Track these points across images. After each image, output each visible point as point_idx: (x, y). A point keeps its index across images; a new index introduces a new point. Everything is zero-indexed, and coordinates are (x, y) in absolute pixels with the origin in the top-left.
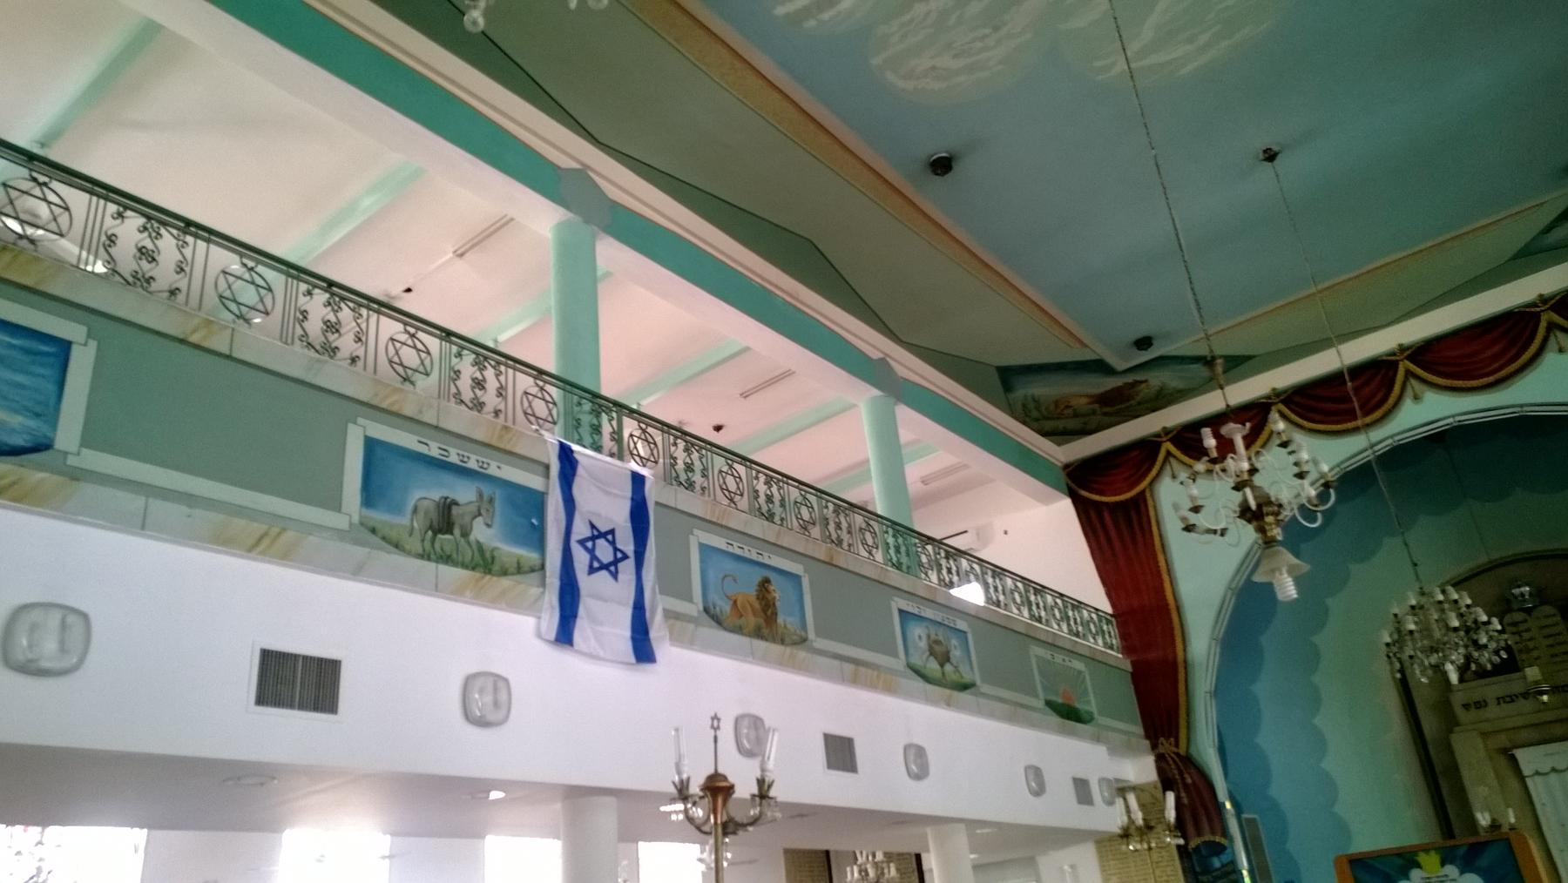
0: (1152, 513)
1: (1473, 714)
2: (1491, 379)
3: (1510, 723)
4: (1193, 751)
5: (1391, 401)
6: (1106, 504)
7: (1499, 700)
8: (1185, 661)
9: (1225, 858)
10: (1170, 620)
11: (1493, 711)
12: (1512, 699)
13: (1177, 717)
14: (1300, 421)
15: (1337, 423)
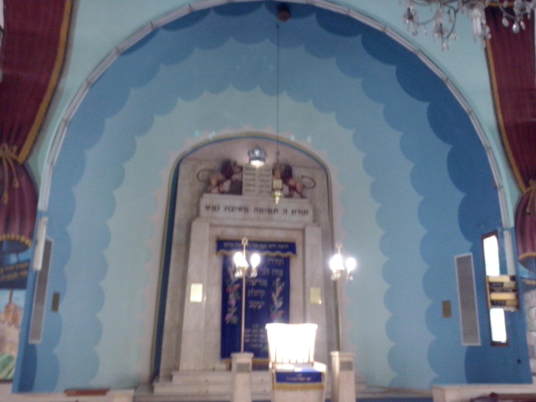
1: (210, 213)
3: (227, 222)
4: (31, 161)
8: (55, 89)
9: (23, 256)
10: (55, 52)
11: (221, 214)
12: (232, 209)
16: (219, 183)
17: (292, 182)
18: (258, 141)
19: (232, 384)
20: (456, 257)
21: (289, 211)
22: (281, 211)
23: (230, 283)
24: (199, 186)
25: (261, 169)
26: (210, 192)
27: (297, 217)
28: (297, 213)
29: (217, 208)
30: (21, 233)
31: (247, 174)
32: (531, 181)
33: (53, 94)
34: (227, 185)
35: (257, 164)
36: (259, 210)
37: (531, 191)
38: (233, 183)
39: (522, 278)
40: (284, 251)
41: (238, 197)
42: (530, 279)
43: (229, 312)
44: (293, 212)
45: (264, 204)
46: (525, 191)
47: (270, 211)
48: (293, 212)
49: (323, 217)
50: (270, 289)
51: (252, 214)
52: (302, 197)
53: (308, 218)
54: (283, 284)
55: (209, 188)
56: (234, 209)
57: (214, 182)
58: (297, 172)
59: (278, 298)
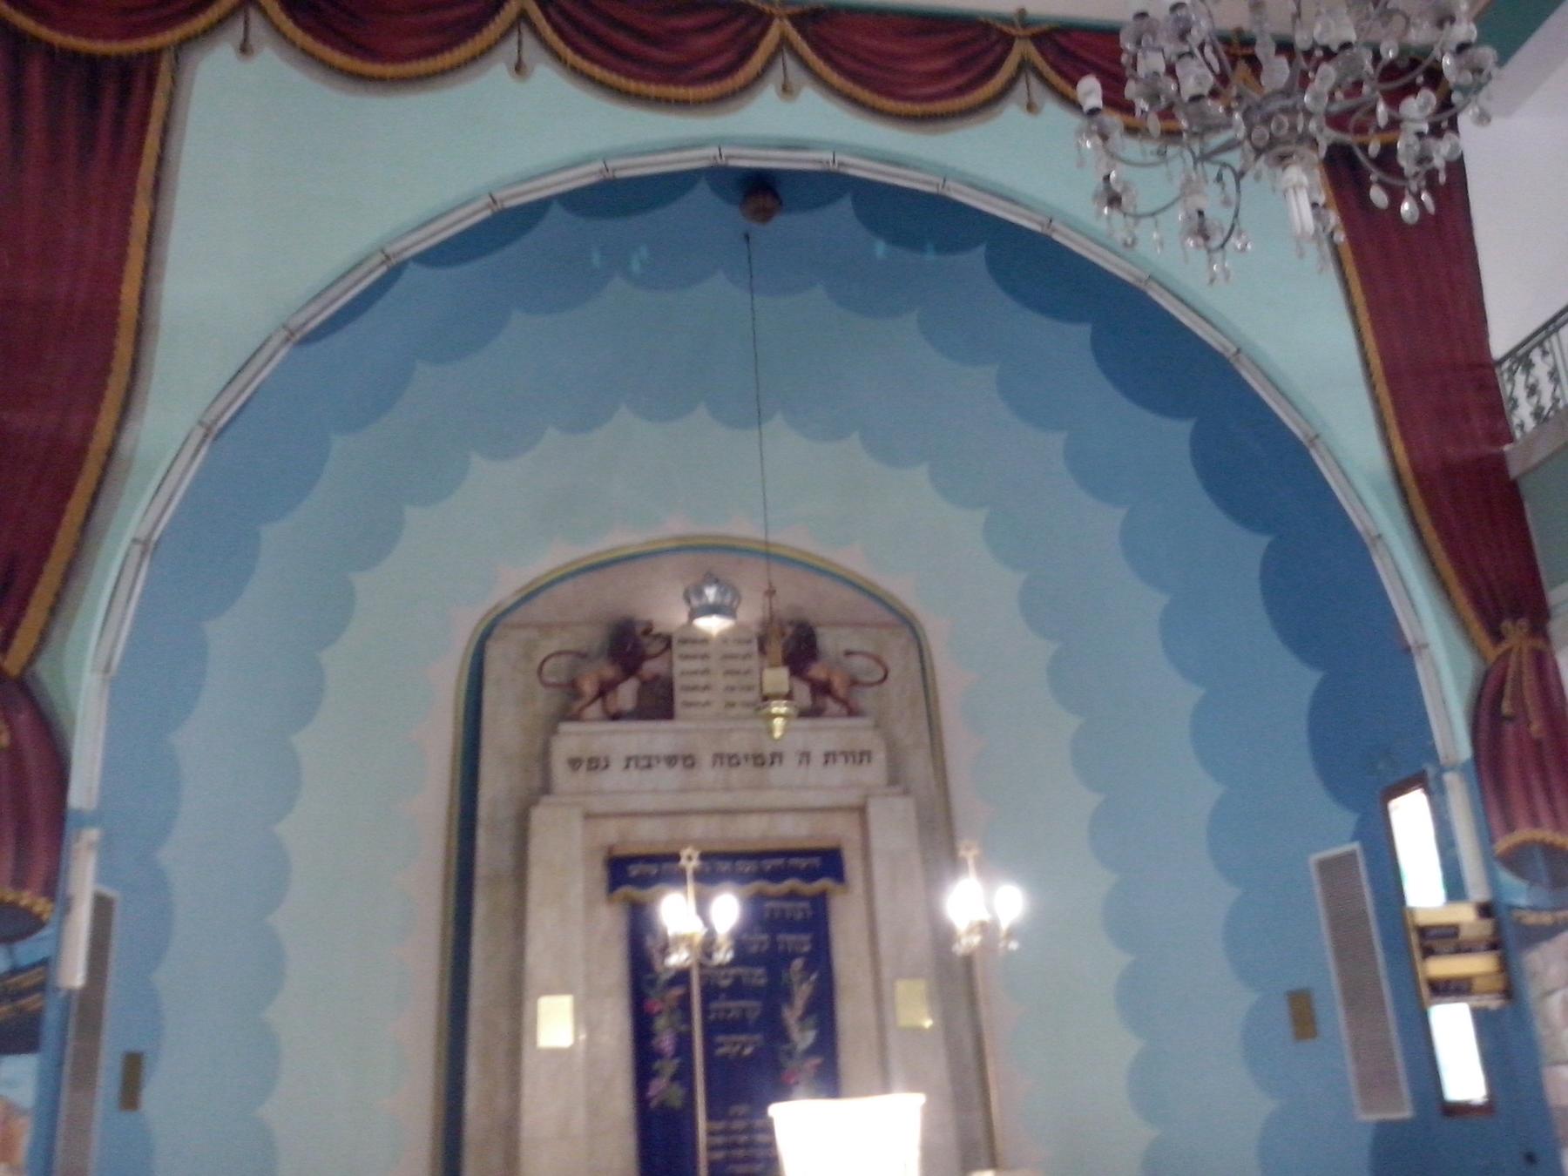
0: (159, 103)
3: (634, 803)
4: (43, 668)
5: (741, 77)
6: (49, 49)
8: (111, 452)
9: (27, 951)
11: (614, 778)
13: (36, 574)
14: (560, 45)
15: (629, 75)
17: (817, 671)
18: (710, 560)
20: (1315, 858)
22: (791, 761)
23: (652, 983)
24: (545, 702)
25: (724, 638)
26: (576, 718)
27: (838, 774)
28: (841, 759)
30: (19, 883)
31: (686, 657)
32: (1507, 625)
33: (105, 468)
34: (627, 694)
35: (712, 625)
36: (728, 760)
37: (1510, 650)
38: (646, 686)
39: (1511, 908)
40: (810, 875)
41: (664, 725)
42: (1534, 909)
43: (655, 1074)
44: (829, 757)
45: (740, 742)
46: (1493, 653)
47: (759, 760)
48: (829, 757)
49: (918, 767)
50: (776, 994)
51: (708, 773)
52: (852, 712)
54: (814, 977)
55: (577, 705)
56: (654, 762)
57: (589, 687)
58: (830, 641)
59: (802, 1019)
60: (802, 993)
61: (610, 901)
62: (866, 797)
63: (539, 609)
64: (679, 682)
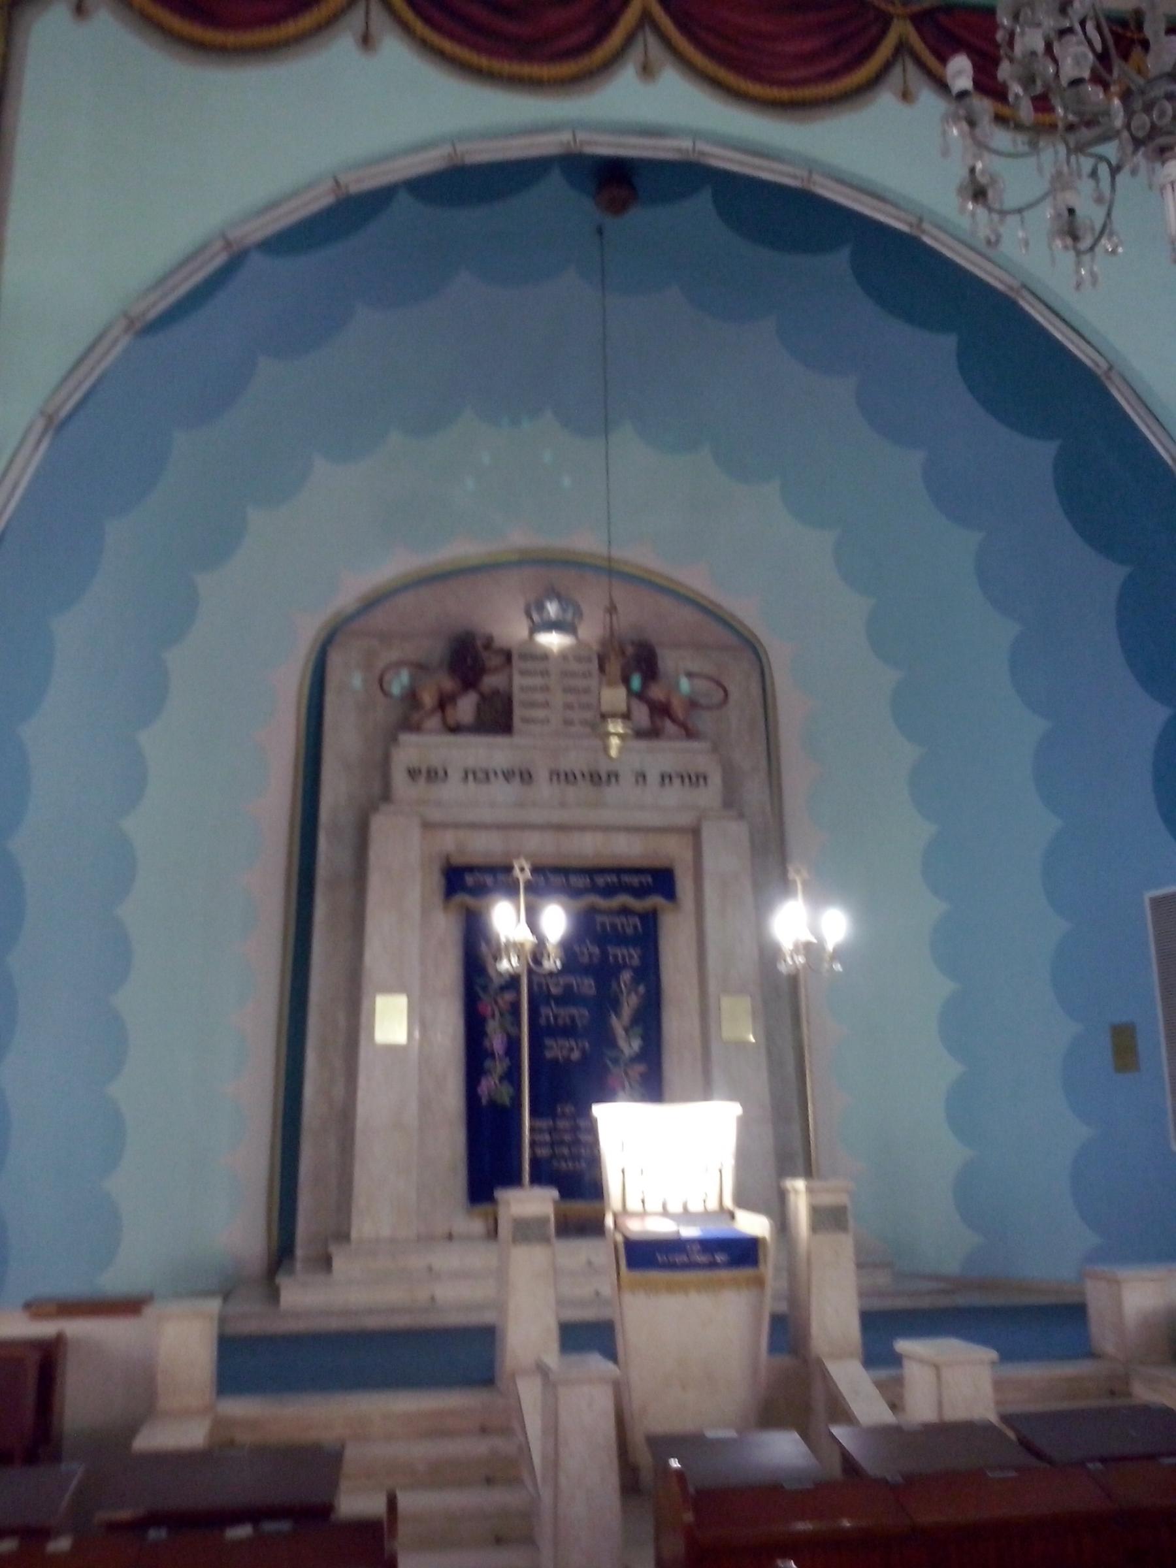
2: (784, 94)
3: (470, 816)
7: (469, 774)
11: (452, 790)
16: (444, 703)
18: (553, 575)
19: (501, 1275)
21: (653, 778)
22: (627, 779)
23: (485, 988)
25: (564, 655)
26: (416, 728)
27: (674, 795)
28: (677, 782)
29: (441, 773)
31: (523, 673)
34: (466, 708)
35: (552, 641)
40: (640, 892)
41: (501, 740)
44: (665, 778)
45: (575, 760)
47: (595, 778)
48: (665, 778)
49: (754, 792)
52: (690, 734)
53: (709, 795)
55: (416, 717)
56: (492, 776)
57: (428, 699)
60: (630, 1003)
61: (446, 908)
62: (699, 820)
63: (379, 619)
64: (518, 697)
